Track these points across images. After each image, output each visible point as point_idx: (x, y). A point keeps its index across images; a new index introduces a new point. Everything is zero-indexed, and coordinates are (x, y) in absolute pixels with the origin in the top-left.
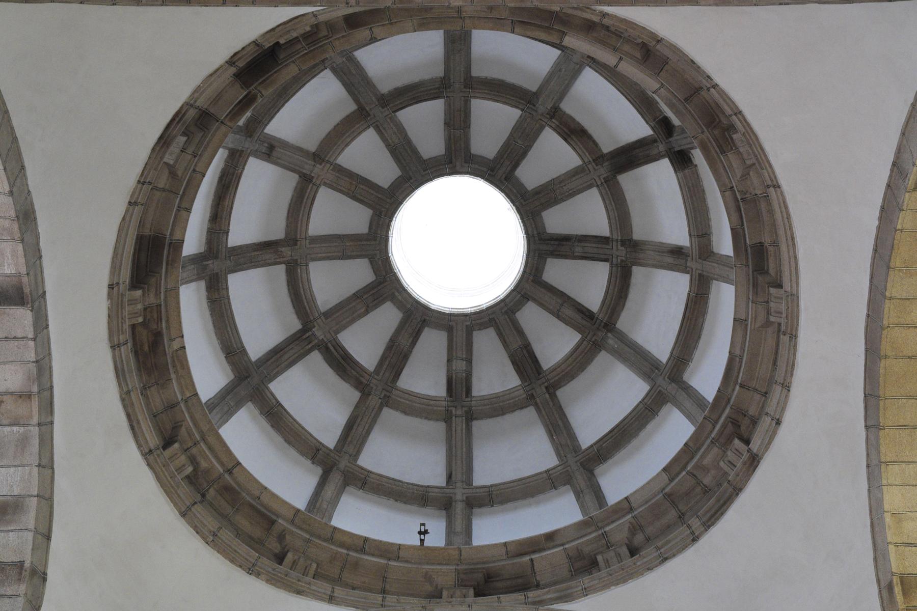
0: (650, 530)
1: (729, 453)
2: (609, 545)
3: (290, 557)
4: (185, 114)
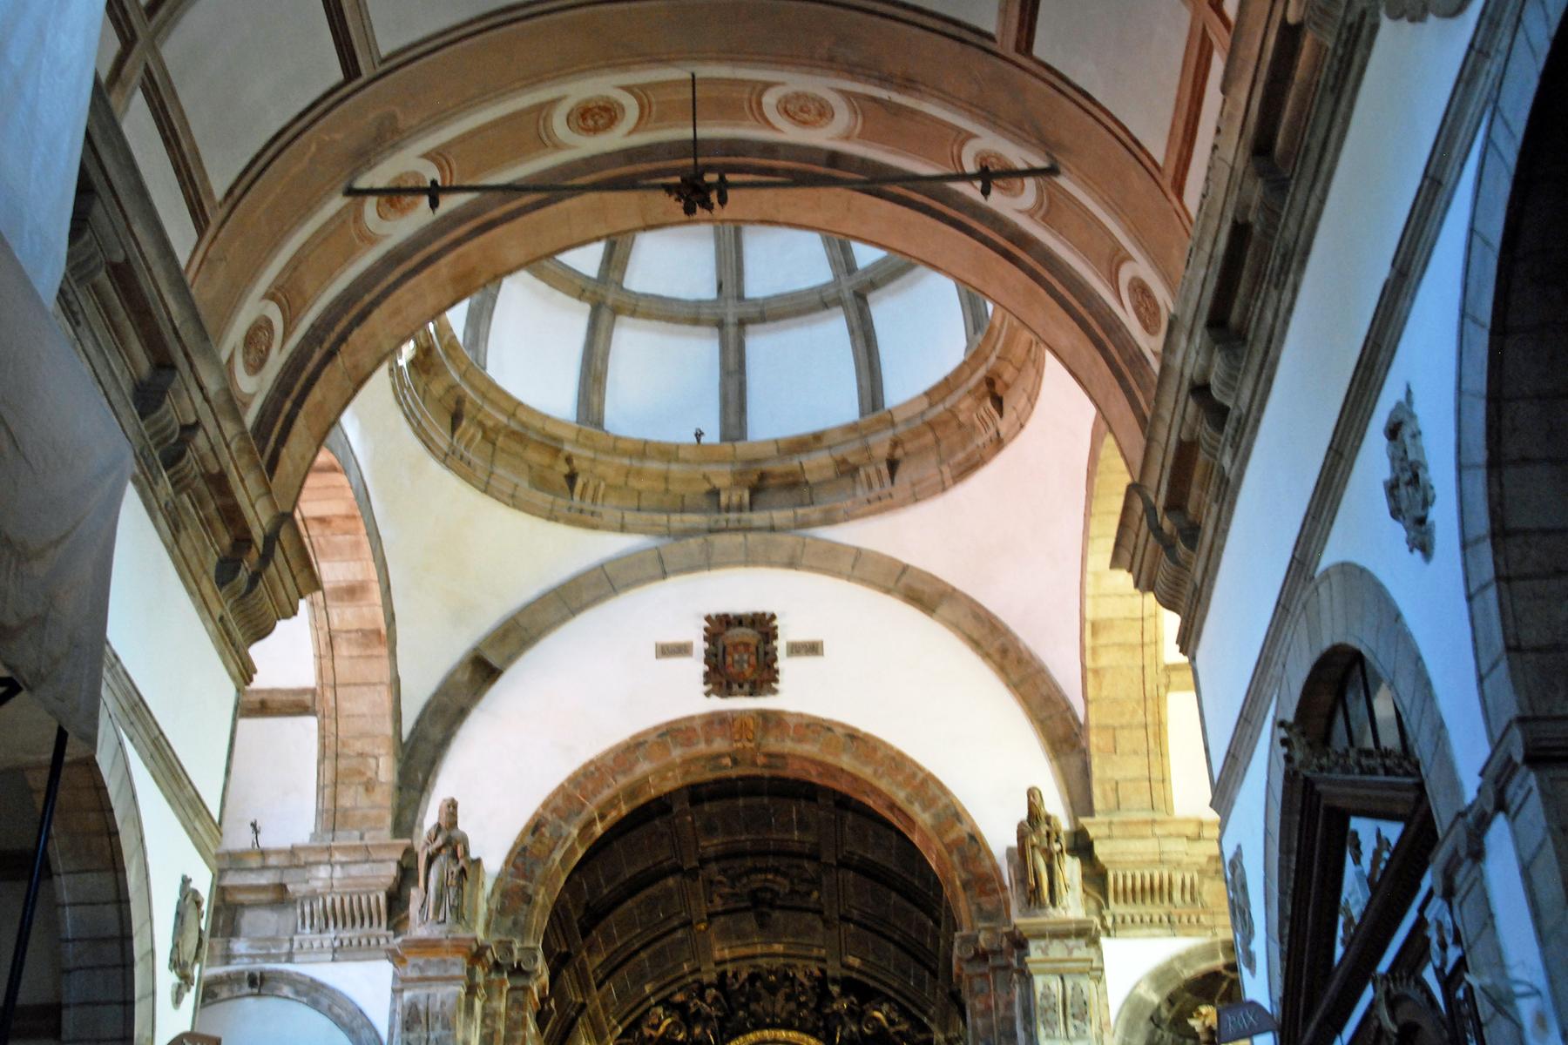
0: (909, 447)
2: (870, 458)
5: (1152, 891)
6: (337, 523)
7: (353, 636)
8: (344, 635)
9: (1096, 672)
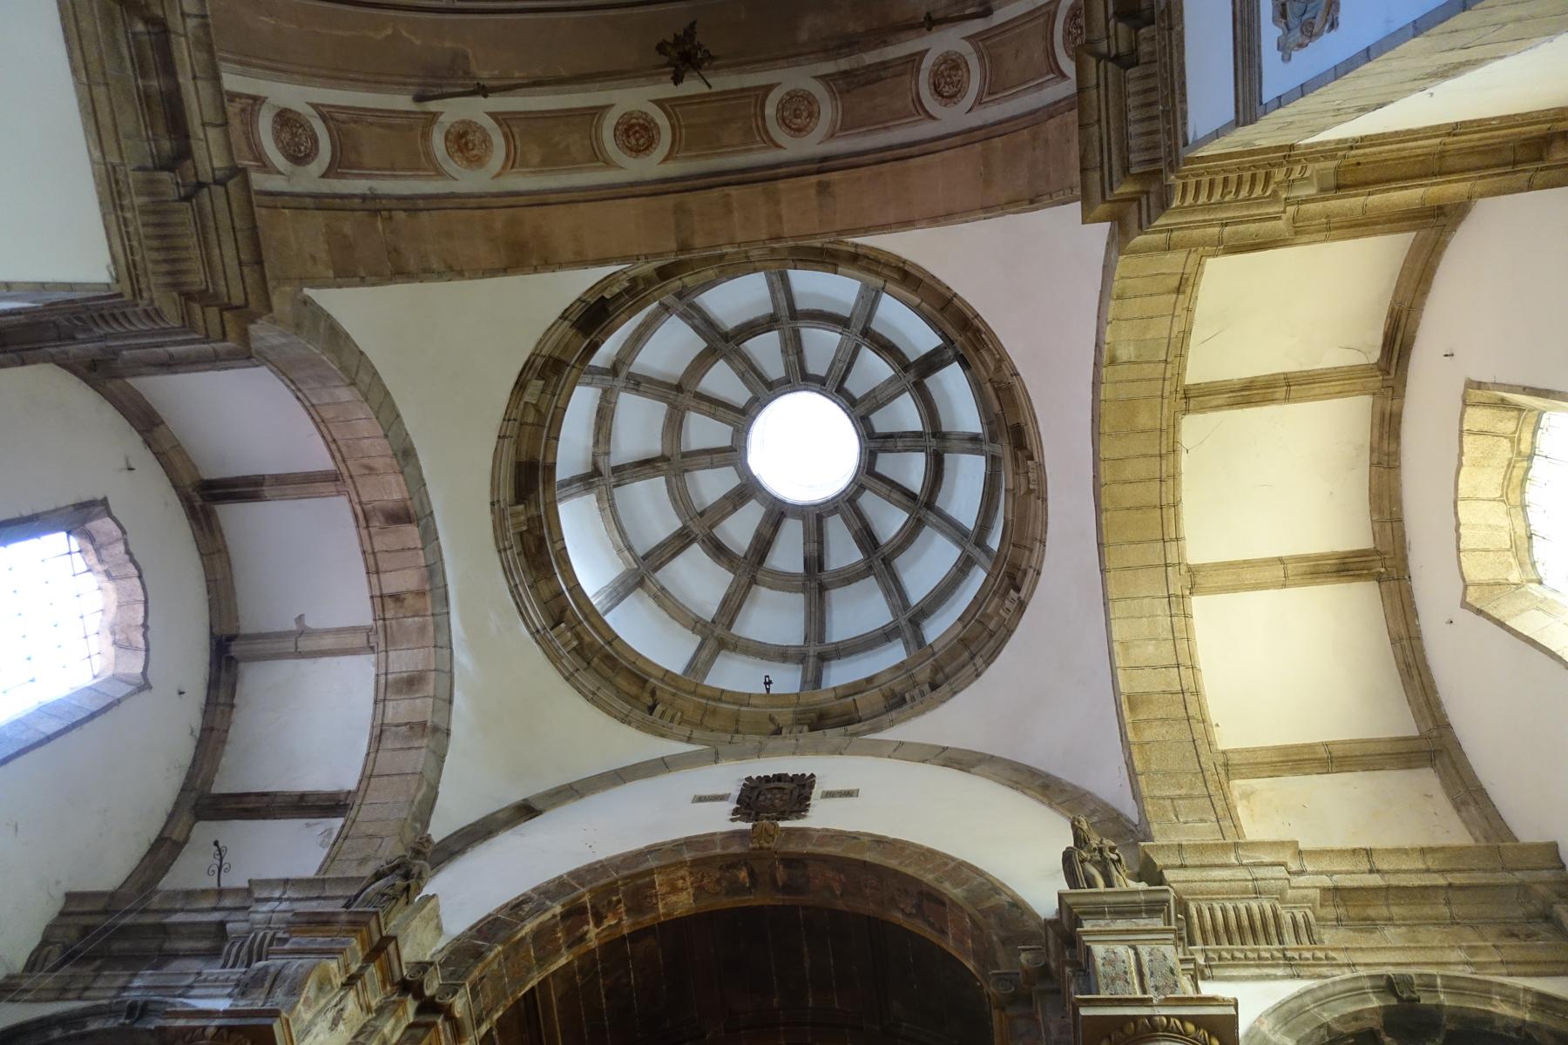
0: (947, 670)
1: (1007, 602)
3: (659, 708)
4: (533, 362)
5: (1257, 929)
6: (410, 601)
7: (403, 729)
8: (393, 729)
9: (1141, 745)
